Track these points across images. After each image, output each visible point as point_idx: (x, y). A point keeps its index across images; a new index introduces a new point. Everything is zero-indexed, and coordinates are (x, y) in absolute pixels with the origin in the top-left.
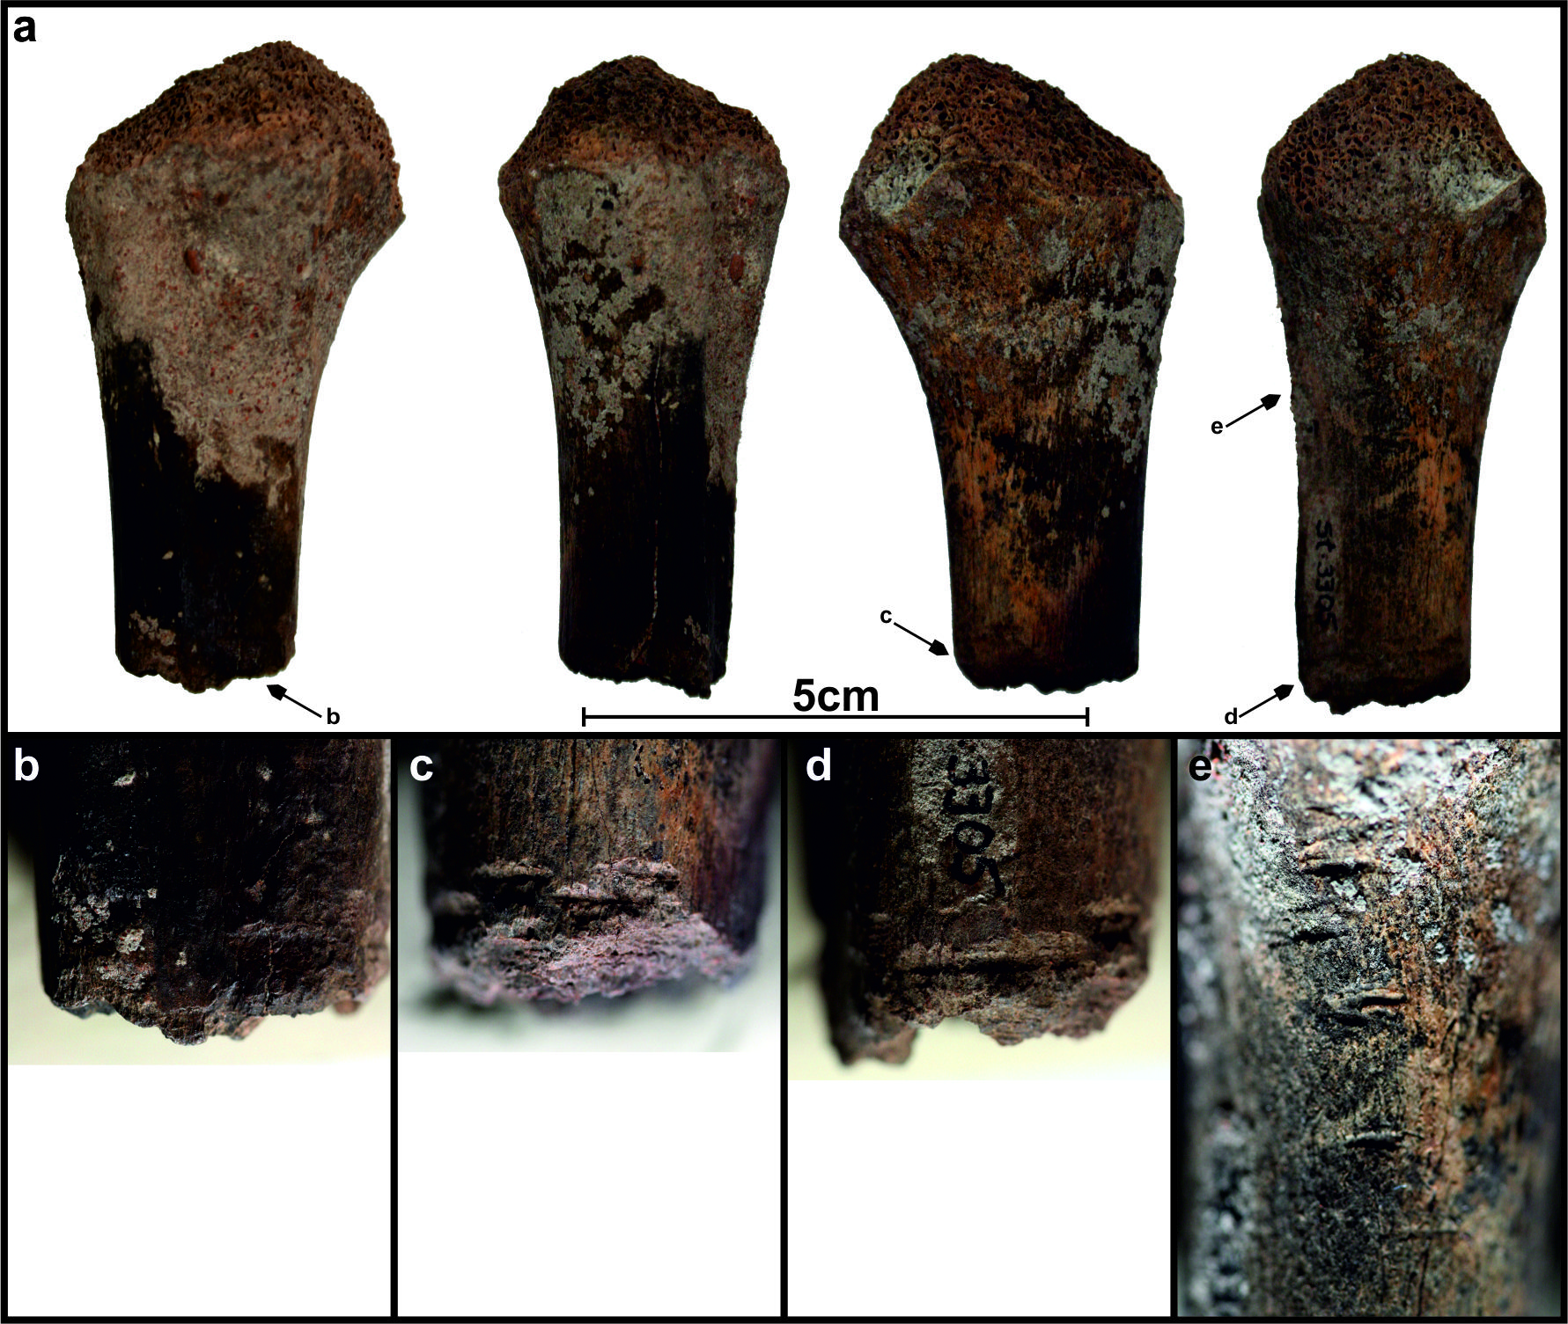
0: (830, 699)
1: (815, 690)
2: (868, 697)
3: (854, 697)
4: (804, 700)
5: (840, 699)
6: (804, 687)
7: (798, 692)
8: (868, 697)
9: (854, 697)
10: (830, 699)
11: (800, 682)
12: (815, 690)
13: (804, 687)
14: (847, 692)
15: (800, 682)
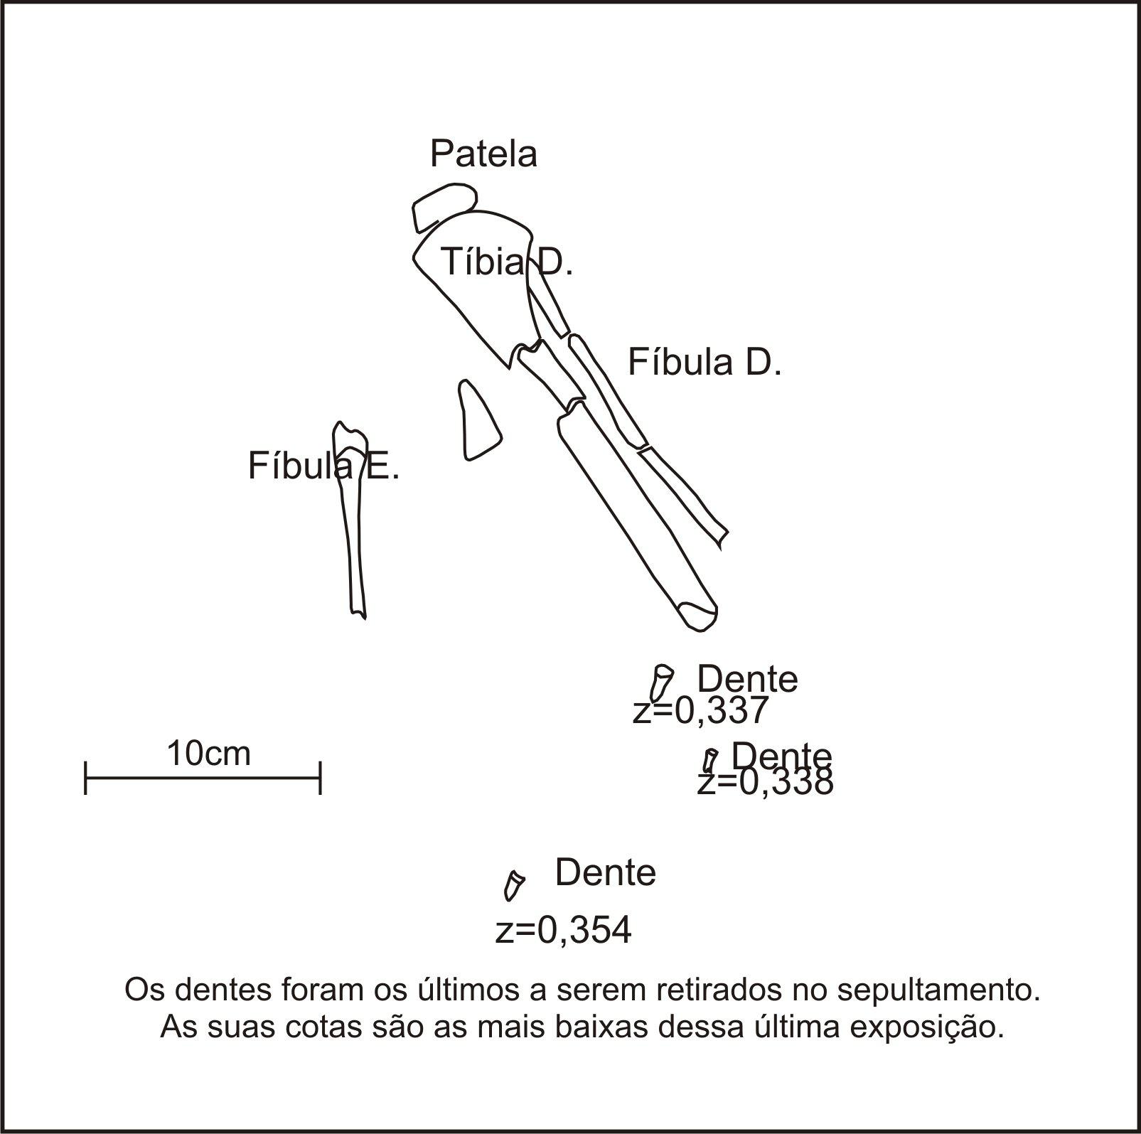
0: (214, 756)
2: (243, 753)
3: (232, 753)
5: (222, 755)
8: (243, 753)
9: (232, 753)
10: (214, 756)
14: (227, 750)
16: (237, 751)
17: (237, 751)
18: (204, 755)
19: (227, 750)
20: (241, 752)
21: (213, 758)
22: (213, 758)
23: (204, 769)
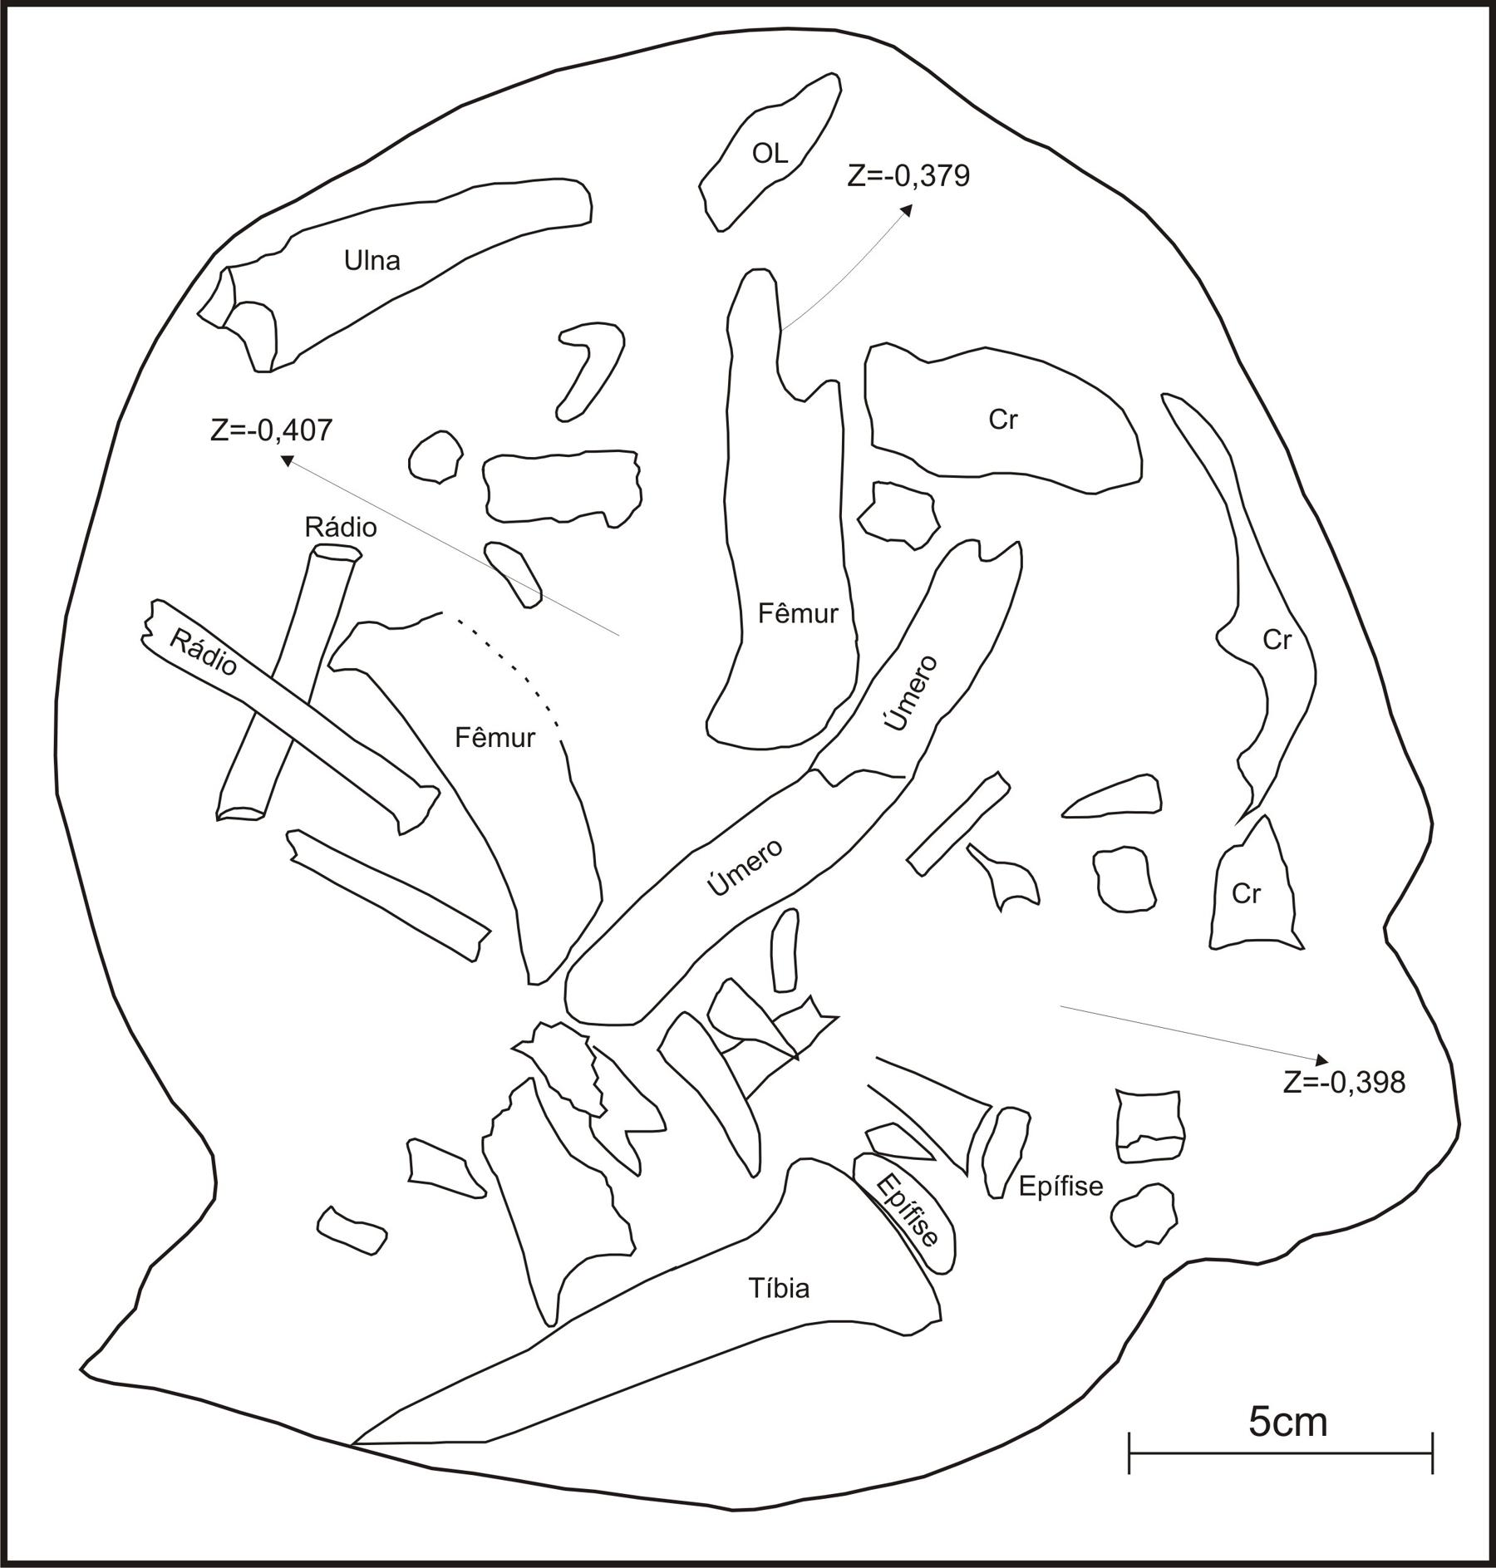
0: (1284, 1425)
1: (1271, 1415)
2: (1318, 1422)
3: (1305, 1422)
4: (1260, 1426)
5: (1293, 1424)
6: (1259, 1413)
7: (1253, 1419)
8: (1318, 1422)
9: (1305, 1422)
10: (1284, 1425)
11: (1255, 1408)
12: (1271, 1415)
13: (1259, 1413)
14: (1299, 1418)
15: (1255, 1408)
16: (1311, 1419)
17: (1311, 1419)
18: (1272, 1426)
19: (1299, 1418)
20: (1316, 1420)
21: (1283, 1428)
22: (1283, 1428)
23: (1272, 1441)
